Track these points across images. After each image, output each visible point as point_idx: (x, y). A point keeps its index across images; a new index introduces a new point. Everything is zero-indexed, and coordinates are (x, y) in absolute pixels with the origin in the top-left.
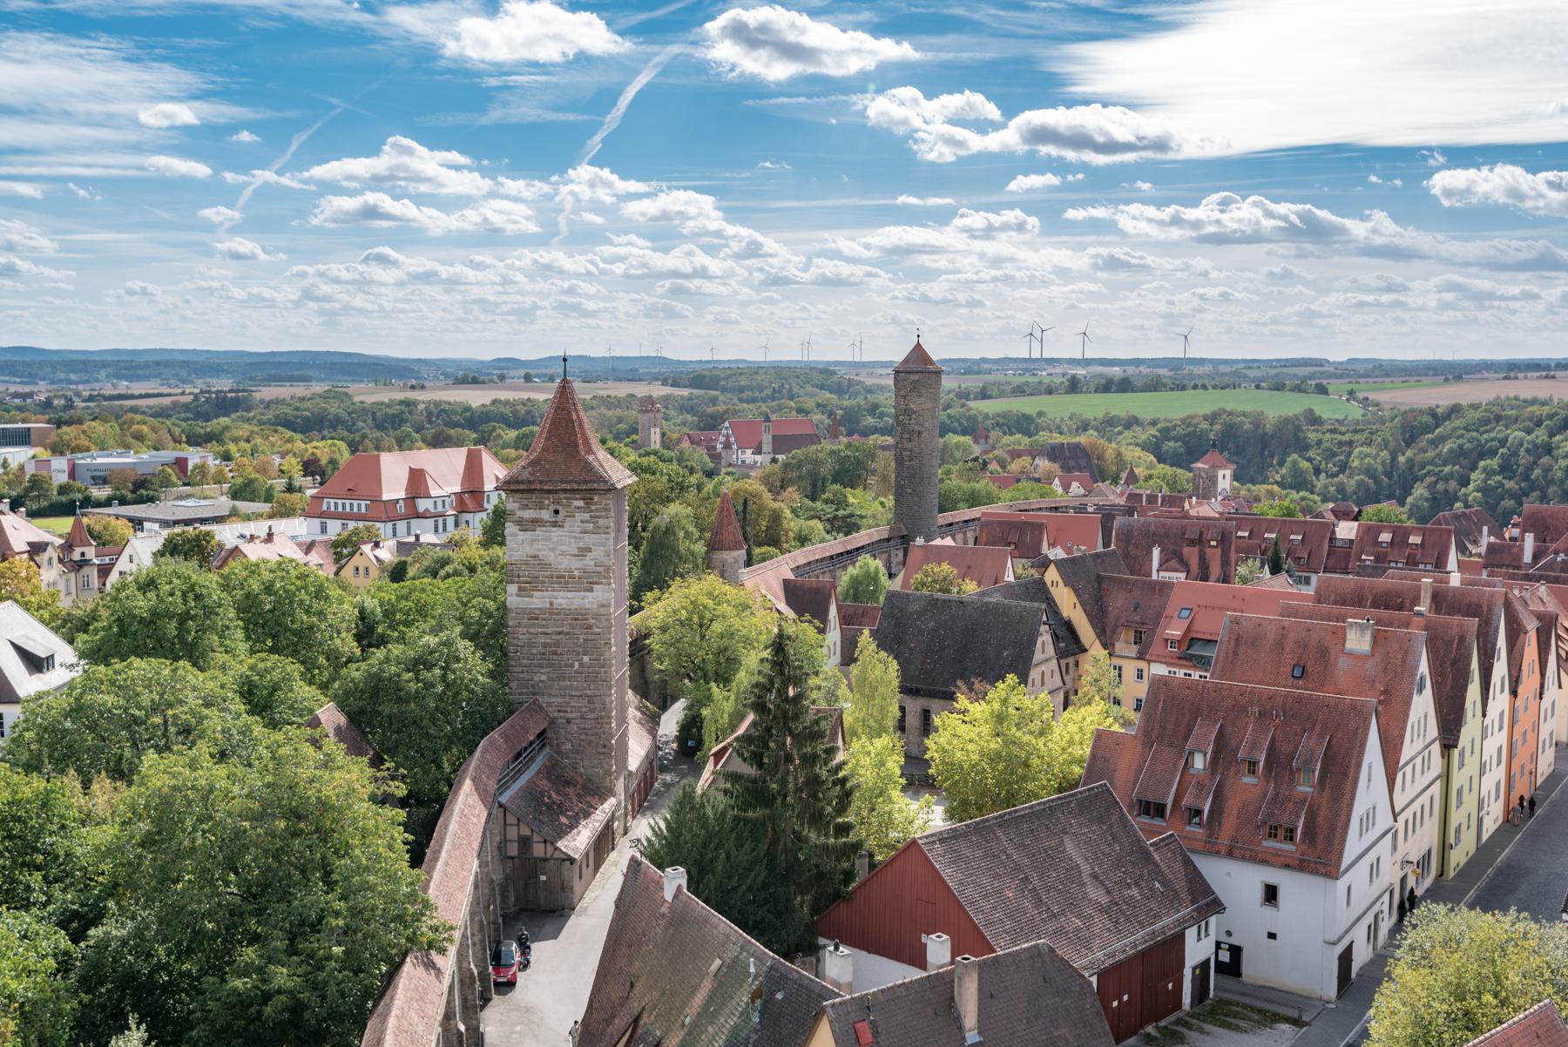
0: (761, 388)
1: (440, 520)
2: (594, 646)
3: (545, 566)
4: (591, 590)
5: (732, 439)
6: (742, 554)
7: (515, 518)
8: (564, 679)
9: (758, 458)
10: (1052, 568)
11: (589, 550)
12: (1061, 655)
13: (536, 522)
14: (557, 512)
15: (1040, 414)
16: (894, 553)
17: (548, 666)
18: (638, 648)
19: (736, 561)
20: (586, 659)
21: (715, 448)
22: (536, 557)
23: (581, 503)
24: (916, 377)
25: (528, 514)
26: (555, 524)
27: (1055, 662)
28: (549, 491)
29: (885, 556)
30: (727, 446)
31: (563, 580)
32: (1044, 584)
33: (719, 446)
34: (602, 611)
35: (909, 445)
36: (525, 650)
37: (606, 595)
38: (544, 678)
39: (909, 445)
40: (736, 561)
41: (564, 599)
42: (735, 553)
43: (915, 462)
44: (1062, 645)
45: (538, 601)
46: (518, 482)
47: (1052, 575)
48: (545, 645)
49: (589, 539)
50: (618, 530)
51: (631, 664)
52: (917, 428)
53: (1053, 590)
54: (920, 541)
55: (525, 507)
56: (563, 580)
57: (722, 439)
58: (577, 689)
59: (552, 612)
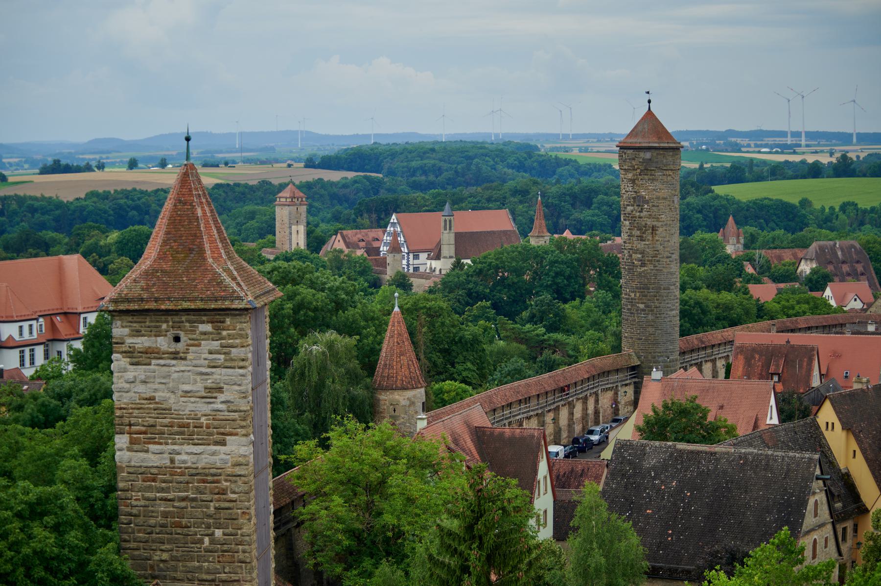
0: (439, 171)
1: (27, 350)
2: (226, 517)
3: (163, 411)
4: (223, 443)
5: (401, 239)
6: (419, 394)
7: (124, 348)
8: (192, 559)
9: (436, 264)
10: (827, 405)
11: (220, 390)
12: (837, 518)
13: (151, 354)
14: (177, 339)
15: (805, 203)
16: (621, 390)
17: (170, 542)
18: (286, 520)
19: (412, 403)
20: (218, 533)
21: (377, 251)
22: (151, 399)
23: (208, 327)
24: (648, 155)
25: (143, 342)
26: (175, 356)
27: (829, 527)
28: (167, 312)
29: (610, 394)
30: (395, 248)
31: (188, 430)
32: (818, 427)
33: (384, 249)
34: (238, 471)
35: (640, 245)
36: (140, 520)
37: (243, 450)
38: (165, 556)
39: (640, 245)
40: (412, 403)
41: (189, 455)
42: (410, 394)
43: (649, 267)
44: (839, 505)
45: (154, 457)
46: (128, 301)
47: (827, 415)
48: (165, 515)
49: (220, 375)
50: (258, 362)
51: (276, 540)
52: (649, 222)
53: (828, 435)
54: (657, 374)
55: (137, 333)
56: (188, 430)
57: (387, 238)
58: (208, 572)
59: (172, 469)
